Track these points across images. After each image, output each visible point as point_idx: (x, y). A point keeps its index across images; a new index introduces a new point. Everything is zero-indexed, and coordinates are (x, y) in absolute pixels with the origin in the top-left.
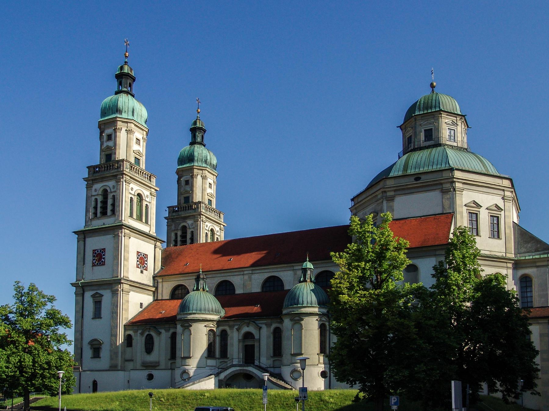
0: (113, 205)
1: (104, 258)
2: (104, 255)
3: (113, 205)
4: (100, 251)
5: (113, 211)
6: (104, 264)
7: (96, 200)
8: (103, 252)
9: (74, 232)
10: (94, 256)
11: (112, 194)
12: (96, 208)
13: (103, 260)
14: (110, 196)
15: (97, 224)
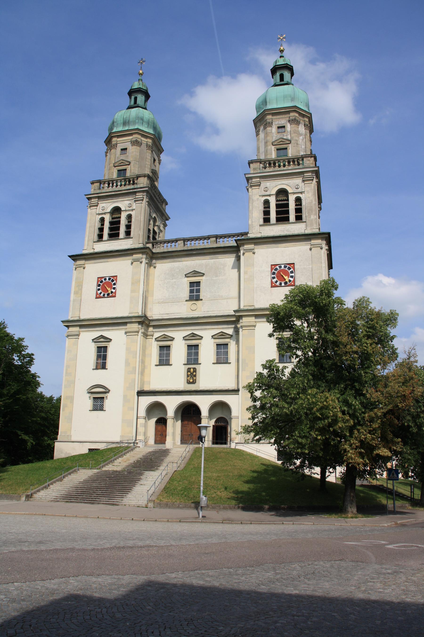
0: (128, 227)
1: (114, 288)
2: (115, 284)
3: (128, 227)
4: (109, 279)
5: (128, 233)
6: (115, 296)
7: (102, 220)
8: (113, 281)
9: (69, 256)
10: (99, 285)
11: (128, 213)
12: (101, 230)
13: (114, 291)
14: (124, 216)
15: (101, 247)
